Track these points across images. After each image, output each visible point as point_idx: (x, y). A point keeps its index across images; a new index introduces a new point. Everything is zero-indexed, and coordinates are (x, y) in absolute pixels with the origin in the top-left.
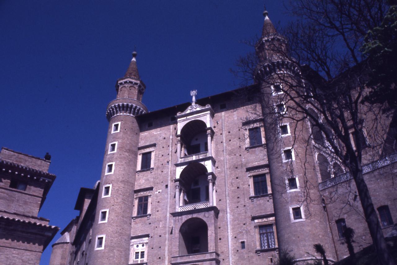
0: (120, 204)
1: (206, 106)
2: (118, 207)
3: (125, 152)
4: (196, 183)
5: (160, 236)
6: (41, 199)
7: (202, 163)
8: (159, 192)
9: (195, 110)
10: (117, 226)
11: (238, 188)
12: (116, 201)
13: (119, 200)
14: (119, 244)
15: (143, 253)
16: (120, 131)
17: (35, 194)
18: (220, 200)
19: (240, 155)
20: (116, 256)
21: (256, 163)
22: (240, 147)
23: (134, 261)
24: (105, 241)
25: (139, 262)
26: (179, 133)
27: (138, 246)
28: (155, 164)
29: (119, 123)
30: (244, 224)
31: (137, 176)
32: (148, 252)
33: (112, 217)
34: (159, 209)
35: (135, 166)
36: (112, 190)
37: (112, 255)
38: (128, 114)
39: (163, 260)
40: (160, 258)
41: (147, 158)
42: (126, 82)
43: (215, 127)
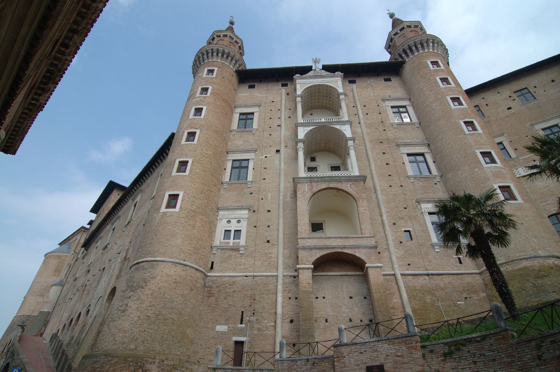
1: (336, 73)
5: (269, 211)
7: (337, 127)
8: (266, 157)
10: (203, 184)
11: (387, 164)
12: (205, 151)
13: (209, 152)
14: (203, 209)
15: (238, 232)
20: (198, 227)
23: (221, 242)
24: (182, 201)
25: (231, 244)
27: (229, 222)
28: (259, 125)
30: (405, 208)
31: (231, 136)
32: (248, 232)
33: (197, 171)
35: (231, 121)
37: (191, 222)
38: (228, 64)
39: (274, 244)
41: (246, 118)
42: (226, 36)
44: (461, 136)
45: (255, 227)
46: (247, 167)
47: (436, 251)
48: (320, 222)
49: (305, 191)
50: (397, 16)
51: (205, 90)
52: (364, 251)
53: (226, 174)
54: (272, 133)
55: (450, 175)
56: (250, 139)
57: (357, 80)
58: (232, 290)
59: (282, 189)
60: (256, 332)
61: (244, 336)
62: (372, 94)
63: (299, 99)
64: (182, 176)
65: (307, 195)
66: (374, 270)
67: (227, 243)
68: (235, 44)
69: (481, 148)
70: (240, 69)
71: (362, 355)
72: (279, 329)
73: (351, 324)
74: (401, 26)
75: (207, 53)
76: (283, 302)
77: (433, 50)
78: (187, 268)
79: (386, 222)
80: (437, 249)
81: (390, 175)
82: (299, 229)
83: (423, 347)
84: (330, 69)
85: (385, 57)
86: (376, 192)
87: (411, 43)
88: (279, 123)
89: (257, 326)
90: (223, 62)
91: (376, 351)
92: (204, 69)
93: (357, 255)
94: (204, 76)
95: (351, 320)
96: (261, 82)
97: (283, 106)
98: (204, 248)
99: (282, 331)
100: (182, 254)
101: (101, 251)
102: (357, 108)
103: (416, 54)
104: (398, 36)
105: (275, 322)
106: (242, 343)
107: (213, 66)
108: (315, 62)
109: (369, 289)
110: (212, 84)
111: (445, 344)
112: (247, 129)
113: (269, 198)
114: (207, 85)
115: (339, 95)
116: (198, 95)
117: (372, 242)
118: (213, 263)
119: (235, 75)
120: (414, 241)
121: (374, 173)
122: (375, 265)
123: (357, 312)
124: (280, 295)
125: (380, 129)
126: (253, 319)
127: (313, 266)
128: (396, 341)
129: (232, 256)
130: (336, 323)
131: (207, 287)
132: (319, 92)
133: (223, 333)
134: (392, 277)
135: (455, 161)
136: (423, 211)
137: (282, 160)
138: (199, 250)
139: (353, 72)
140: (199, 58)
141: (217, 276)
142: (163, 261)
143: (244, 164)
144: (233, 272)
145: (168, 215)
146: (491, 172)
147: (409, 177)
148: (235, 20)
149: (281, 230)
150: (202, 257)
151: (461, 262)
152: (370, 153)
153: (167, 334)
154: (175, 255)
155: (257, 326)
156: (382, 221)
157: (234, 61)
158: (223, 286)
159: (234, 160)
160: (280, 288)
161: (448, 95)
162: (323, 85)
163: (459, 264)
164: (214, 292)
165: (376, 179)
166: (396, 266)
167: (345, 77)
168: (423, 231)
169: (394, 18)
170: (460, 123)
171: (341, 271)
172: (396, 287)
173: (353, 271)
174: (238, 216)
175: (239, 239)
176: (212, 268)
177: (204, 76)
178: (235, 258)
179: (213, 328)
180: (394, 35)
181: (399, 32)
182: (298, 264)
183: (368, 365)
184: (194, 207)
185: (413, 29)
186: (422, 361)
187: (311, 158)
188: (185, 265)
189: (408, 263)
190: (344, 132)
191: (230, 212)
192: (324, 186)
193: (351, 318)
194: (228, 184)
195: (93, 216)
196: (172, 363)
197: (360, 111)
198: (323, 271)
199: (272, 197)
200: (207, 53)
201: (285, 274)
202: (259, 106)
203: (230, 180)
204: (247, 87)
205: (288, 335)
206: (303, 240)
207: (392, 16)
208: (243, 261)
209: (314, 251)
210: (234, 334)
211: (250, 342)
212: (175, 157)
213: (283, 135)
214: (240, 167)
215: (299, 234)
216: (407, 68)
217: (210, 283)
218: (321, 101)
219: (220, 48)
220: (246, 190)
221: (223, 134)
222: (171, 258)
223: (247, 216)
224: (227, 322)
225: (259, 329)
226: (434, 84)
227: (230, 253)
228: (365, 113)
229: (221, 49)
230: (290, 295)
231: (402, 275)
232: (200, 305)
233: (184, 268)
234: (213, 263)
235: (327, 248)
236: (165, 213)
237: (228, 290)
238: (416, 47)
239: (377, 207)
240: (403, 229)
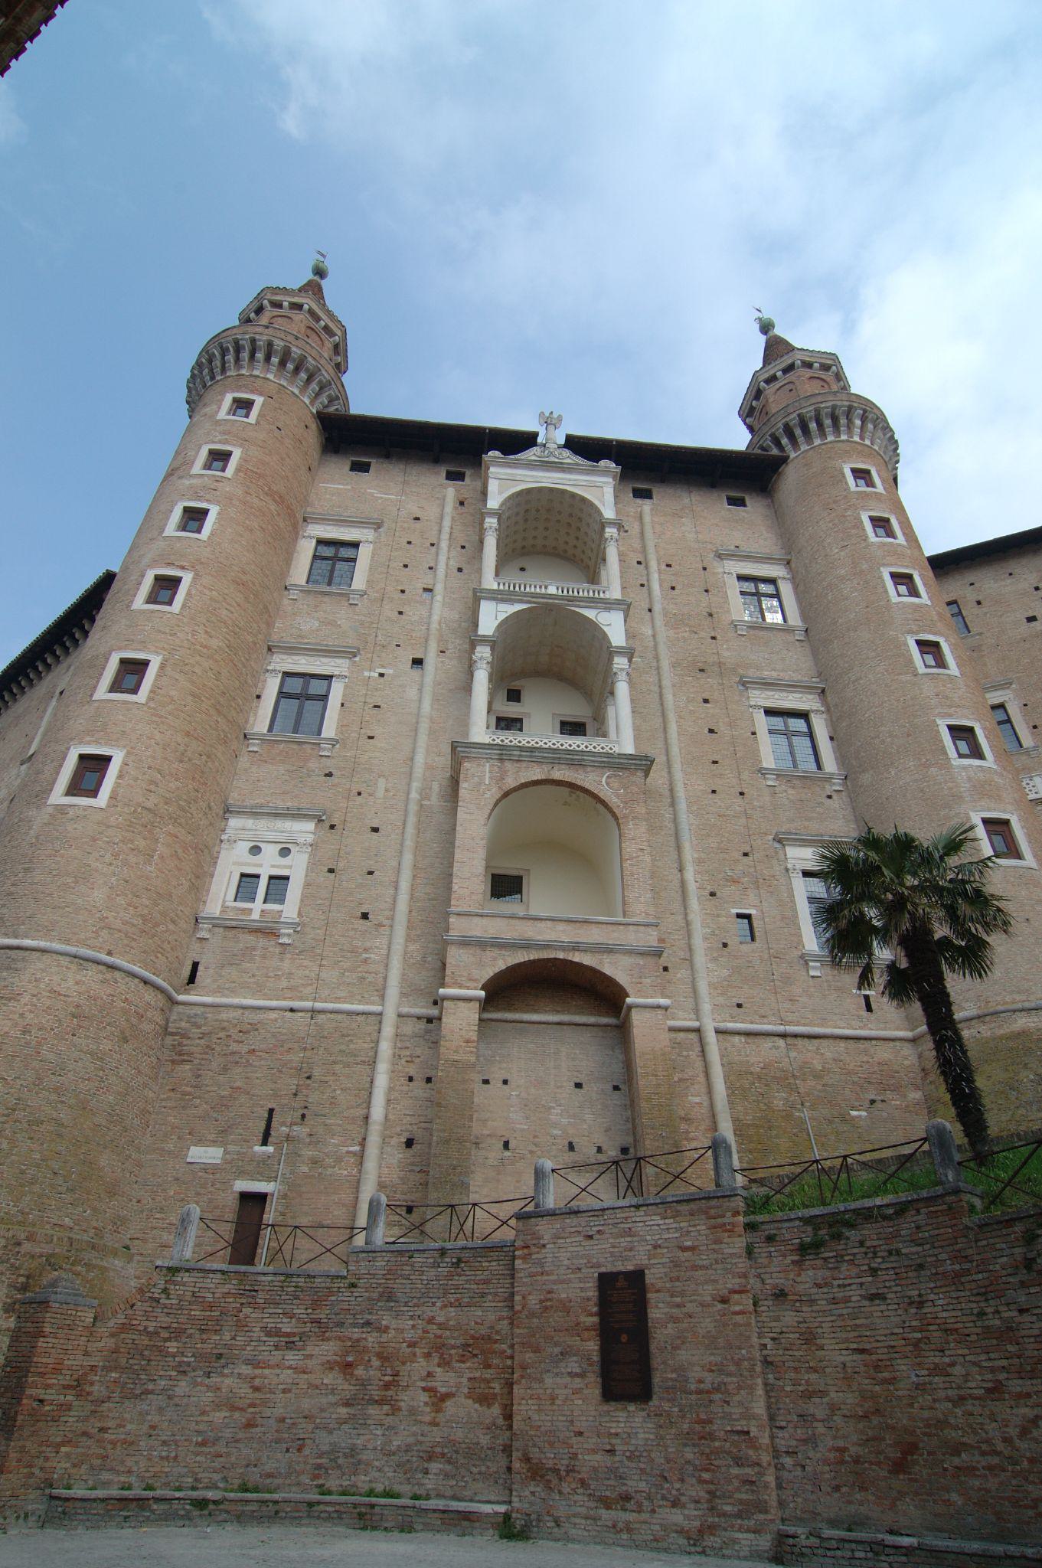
0: (217, 657)
1: (602, 463)
5: (375, 830)
8: (382, 675)
10: (188, 734)
11: (711, 731)
12: (202, 637)
13: (215, 643)
15: (279, 882)
16: (258, 423)
20: (162, 857)
22: (711, 615)
23: (225, 908)
24: (120, 776)
25: (256, 916)
26: (493, 503)
27: (255, 850)
30: (746, 854)
31: (286, 602)
32: (307, 884)
33: (173, 693)
34: (377, 731)
36: (189, 594)
37: (141, 843)
38: (296, 391)
39: (381, 925)
41: (336, 555)
44: (909, 677)
45: (331, 871)
46: (324, 698)
47: (812, 973)
48: (515, 873)
49: (481, 785)
50: (778, 331)
51: (219, 457)
52: (626, 961)
53: (261, 712)
54: (405, 609)
55: (866, 778)
56: (341, 619)
57: (656, 491)
58: (245, 1048)
59: (419, 770)
60: (305, 1169)
61: (269, 1179)
62: (691, 536)
63: (491, 522)
64: (125, 702)
65: (488, 795)
66: (648, 1014)
67: (243, 910)
68: (324, 336)
69: (950, 716)
70: (331, 409)
71: (592, 1242)
72: (371, 1165)
73: (569, 1158)
74: (786, 361)
75: (238, 349)
76: (391, 1089)
78: (117, 974)
79: (692, 887)
80: (814, 968)
82: (455, 887)
83: (750, 1227)
85: (736, 438)
86: (673, 804)
87: (808, 411)
88: (427, 581)
89: (308, 1153)
91: (629, 1233)
92: (223, 394)
93: (608, 970)
94: (222, 414)
95: (571, 1147)
96: (387, 456)
97: (445, 536)
98: (173, 922)
99: (379, 1168)
100: (104, 933)
102: (647, 567)
103: (817, 442)
104: (776, 385)
105: (363, 1143)
106: (261, 1198)
107: (252, 392)
109: (628, 1065)
110: (243, 442)
111: (807, 1221)
112: (334, 589)
113: (380, 793)
114: (226, 442)
115: (603, 526)
116: (197, 468)
117: (649, 939)
118: (195, 965)
119: (314, 426)
120: (757, 944)
121: (675, 750)
122: (650, 1001)
123: (591, 1126)
124: (383, 1068)
125: (702, 634)
126: (300, 1131)
127: (483, 993)
128: (684, 1207)
129: (254, 949)
130: (531, 1152)
131: (172, 1034)
132: (548, 510)
133: (207, 1168)
134: (693, 1036)
135: (883, 742)
136: (789, 866)
137: (428, 690)
138: (157, 925)
139: (648, 467)
140: (210, 361)
141: (204, 1005)
142: (44, 951)
143: (316, 687)
144: (253, 996)
145: (69, 816)
146: (969, 780)
147: (763, 772)
148: (329, 264)
149: (405, 885)
150: (166, 946)
151: (869, 1008)
152: (669, 698)
153: (38, 1166)
154: (82, 936)
155: (308, 1153)
156: (683, 884)
157: (314, 386)
158: (222, 1035)
159: (287, 674)
160: (385, 1048)
161: (884, 565)
162: (564, 492)
163: (864, 1013)
164: (193, 1049)
165: (677, 767)
166: (706, 1007)
167: (624, 477)
168: (783, 918)
169: (771, 334)
170: (906, 644)
171: (558, 1012)
172: (699, 1064)
173: (591, 1014)
175: (282, 901)
176: (192, 979)
177: (222, 414)
178: (264, 957)
179: (180, 1154)
180: (768, 381)
181: (779, 374)
182: (443, 985)
183: (603, 1270)
186: (742, 1264)
187: (509, 691)
188: (112, 967)
189: (736, 1001)
190: (605, 629)
192: (536, 773)
193: (575, 1140)
194: (263, 740)
196: (46, 1249)
197: (655, 577)
198: (510, 1007)
199: (387, 790)
200: (238, 349)
201: (405, 1010)
202: (378, 526)
203: (270, 730)
205: (397, 1181)
206: (463, 919)
207: (766, 327)
208: (286, 965)
209: (491, 953)
210: (242, 1174)
211: (285, 1197)
212: (106, 647)
213: (435, 618)
214: (304, 695)
215: (453, 902)
216: (791, 478)
217: (183, 1024)
218: (551, 534)
219: (277, 342)
220: (313, 765)
221: (262, 593)
222: (68, 942)
223: (310, 838)
224: (221, 1138)
225: (315, 1162)
227: (250, 939)
228: (667, 586)
229: (278, 344)
230: (412, 1070)
231: (718, 1031)
232: (145, 1085)
233: (108, 976)
234: (195, 965)
235: (527, 946)
236: (61, 809)
237: (234, 1047)
238: (820, 425)
239: (673, 844)
240: (735, 911)
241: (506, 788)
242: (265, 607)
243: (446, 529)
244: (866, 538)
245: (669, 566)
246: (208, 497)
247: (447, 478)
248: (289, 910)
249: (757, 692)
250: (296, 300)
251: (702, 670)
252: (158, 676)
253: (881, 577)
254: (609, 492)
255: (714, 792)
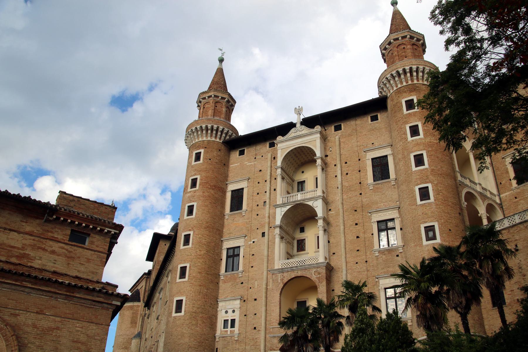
1: (315, 127)
2: (201, 261)
3: (210, 189)
4: (302, 230)
5: (255, 300)
6: (106, 256)
7: (310, 203)
8: (254, 242)
9: (300, 133)
10: (200, 286)
11: (358, 237)
13: (202, 252)
14: (203, 309)
17: (98, 249)
18: (334, 254)
19: (361, 194)
21: (382, 204)
22: (360, 183)
24: (186, 305)
26: (279, 163)
27: (226, 312)
29: (202, 151)
31: (225, 220)
32: (240, 321)
36: (193, 239)
38: (213, 139)
39: (259, 331)
40: (255, 328)
42: (209, 97)
43: (326, 156)
45: (245, 315)
46: (238, 255)
54: (259, 213)
70: (228, 137)
77: (412, 80)
81: (358, 250)
84: (310, 122)
90: (209, 139)
97: (269, 177)
101: (156, 321)
108: (298, 111)
110: (199, 171)
114: (195, 175)
118: (217, 349)
119: (223, 147)
129: (229, 342)
136: (380, 288)
159: (228, 249)
161: (412, 152)
162: (303, 147)
174: (233, 307)
181: (387, 46)
184: (195, 309)
185: (400, 41)
187: (301, 228)
191: (228, 303)
195: (149, 265)
199: (258, 285)
203: (226, 271)
204: (238, 153)
208: (237, 345)
214: (233, 254)
226: (403, 136)
236: (174, 317)
241: (285, 282)
242: (218, 230)
243: (269, 174)
244: (406, 139)
245: (346, 163)
246: (193, 200)
247: (270, 147)
248: (236, 329)
249: (374, 215)
250: (209, 94)
251: (356, 211)
252: (189, 270)
253: (410, 159)
254: (318, 143)
255: (357, 263)
